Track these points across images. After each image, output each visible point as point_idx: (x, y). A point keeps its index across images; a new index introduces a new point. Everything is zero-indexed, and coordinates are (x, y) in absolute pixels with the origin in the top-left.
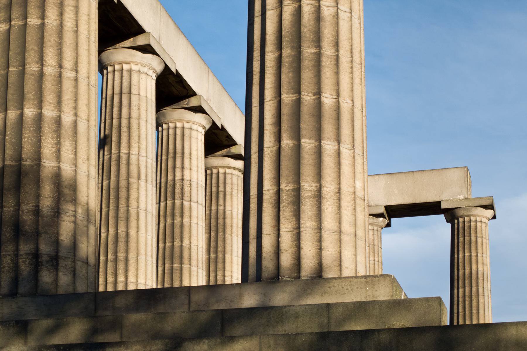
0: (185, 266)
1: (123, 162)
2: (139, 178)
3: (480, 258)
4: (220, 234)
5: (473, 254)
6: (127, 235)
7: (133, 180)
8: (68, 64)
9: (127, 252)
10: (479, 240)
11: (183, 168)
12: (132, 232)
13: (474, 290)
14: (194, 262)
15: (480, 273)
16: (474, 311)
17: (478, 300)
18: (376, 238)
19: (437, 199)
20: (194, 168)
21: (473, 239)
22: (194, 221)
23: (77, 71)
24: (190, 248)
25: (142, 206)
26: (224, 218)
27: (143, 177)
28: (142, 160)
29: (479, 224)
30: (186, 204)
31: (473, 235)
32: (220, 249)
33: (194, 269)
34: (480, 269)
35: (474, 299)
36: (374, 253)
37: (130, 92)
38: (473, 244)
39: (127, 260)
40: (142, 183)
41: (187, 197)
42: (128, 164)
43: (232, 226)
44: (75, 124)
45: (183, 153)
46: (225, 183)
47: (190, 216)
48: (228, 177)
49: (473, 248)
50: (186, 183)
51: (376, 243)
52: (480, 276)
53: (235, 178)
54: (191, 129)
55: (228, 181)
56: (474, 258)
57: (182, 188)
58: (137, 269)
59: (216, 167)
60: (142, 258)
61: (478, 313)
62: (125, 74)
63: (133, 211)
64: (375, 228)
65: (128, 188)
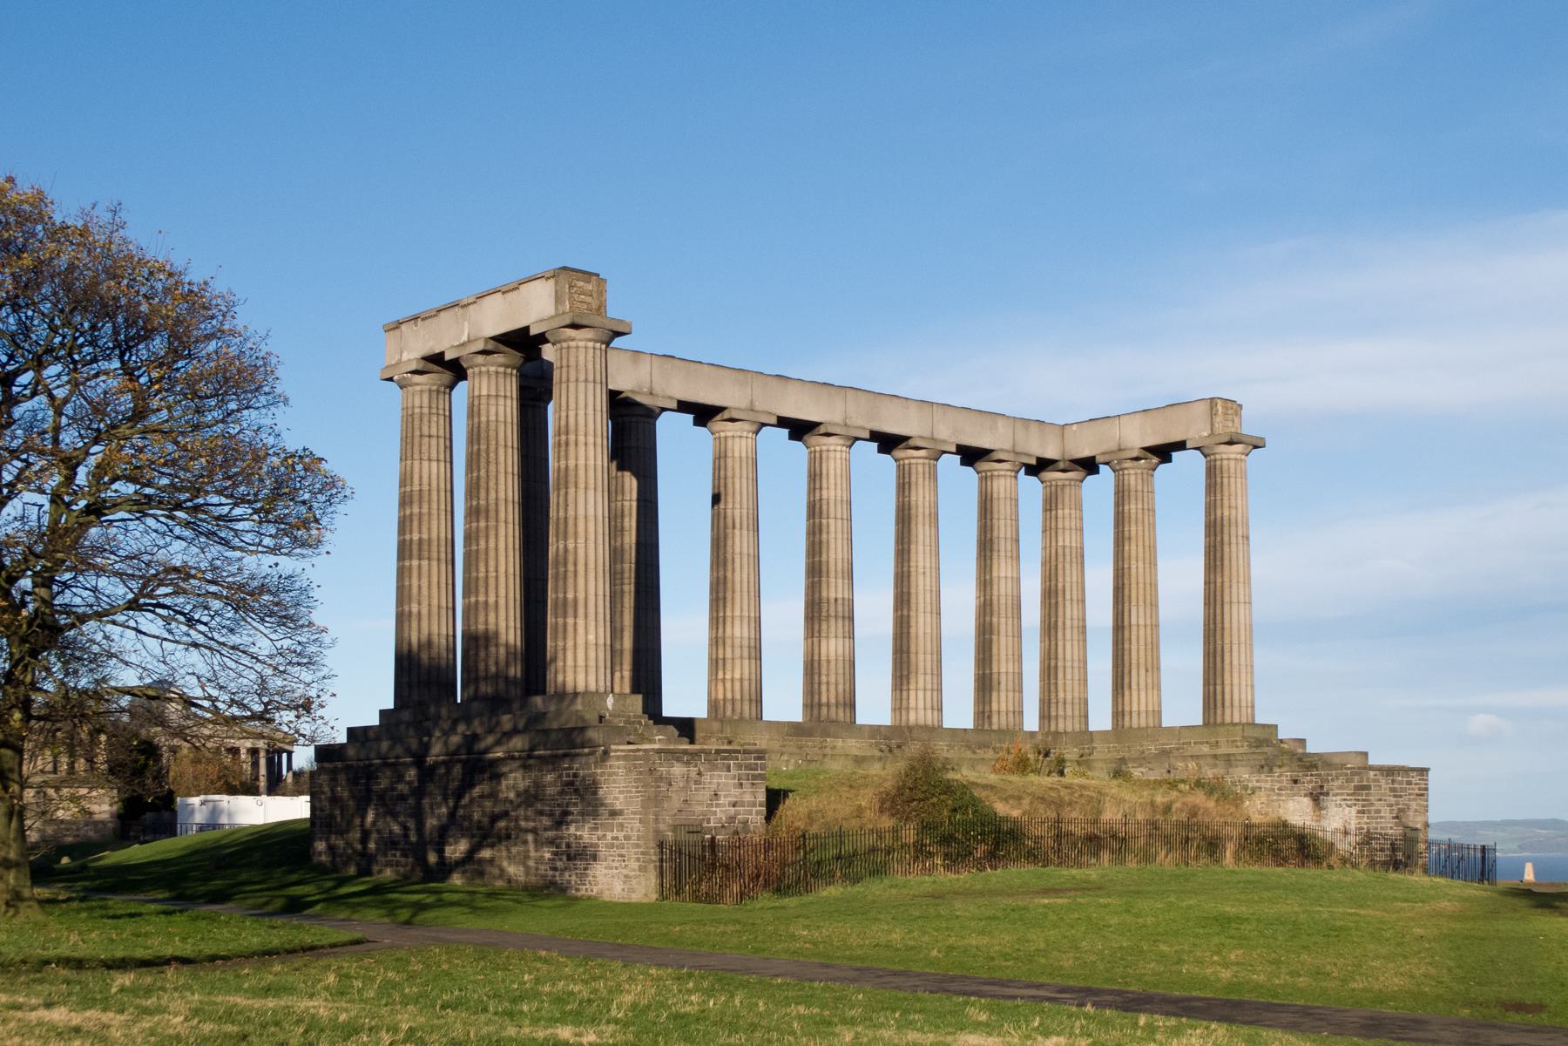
0: (824, 579)
1: (722, 516)
2: (734, 527)
3: (1226, 502)
4: (906, 524)
5: (1219, 498)
6: (725, 577)
7: (729, 531)
8: (492, 569)
9: (725, 593)
10: (1226, 480)
11: (821, 488)
12: (729, 575)
13: (1219, 539)
14: (832, 574)
15: (1226, 519)
16: (1218, 563)
17: (1222, 550)
18: (1140, 481)
20: (832, 487)
21: (1219, 480)
22: (832, 535)
23: (497, 571)
24: (828, 562)
25: (737, 550)
26: (909, 509)
27: (738, 526)
28: (737, 513)
29: (1225, 462)
30: (824, 521)
31: (1219, 476)
32: (906, 540)
33: (832, 580)
34: (1226, 513)
35: (1219, 549)
36: (1136, 500)
37: (726, 456)
38: (1218, 486)
39: (725, 598)
40: (737, 532)
41: (825, 515)
42: (725, 517)
43: (917, 516)
44: (497, 602)
45: (821, 475)
46: (910, 473)
47: (828, 533)
48: (913, 467)
49: (1218, 491)
50: (824, 502)
51: (1140, 488)
52: (1226, 523)
53: (920, 469)
54: (828, 451)
55: (913, 471)
56: (1219, 502)
57: (821, 507)
58: (733, 604)
59: (903, 459)
61: (1222, 565)
62: (722, 440)
63: (729, 556)
64: (1139, 471)
65: (725, 538)
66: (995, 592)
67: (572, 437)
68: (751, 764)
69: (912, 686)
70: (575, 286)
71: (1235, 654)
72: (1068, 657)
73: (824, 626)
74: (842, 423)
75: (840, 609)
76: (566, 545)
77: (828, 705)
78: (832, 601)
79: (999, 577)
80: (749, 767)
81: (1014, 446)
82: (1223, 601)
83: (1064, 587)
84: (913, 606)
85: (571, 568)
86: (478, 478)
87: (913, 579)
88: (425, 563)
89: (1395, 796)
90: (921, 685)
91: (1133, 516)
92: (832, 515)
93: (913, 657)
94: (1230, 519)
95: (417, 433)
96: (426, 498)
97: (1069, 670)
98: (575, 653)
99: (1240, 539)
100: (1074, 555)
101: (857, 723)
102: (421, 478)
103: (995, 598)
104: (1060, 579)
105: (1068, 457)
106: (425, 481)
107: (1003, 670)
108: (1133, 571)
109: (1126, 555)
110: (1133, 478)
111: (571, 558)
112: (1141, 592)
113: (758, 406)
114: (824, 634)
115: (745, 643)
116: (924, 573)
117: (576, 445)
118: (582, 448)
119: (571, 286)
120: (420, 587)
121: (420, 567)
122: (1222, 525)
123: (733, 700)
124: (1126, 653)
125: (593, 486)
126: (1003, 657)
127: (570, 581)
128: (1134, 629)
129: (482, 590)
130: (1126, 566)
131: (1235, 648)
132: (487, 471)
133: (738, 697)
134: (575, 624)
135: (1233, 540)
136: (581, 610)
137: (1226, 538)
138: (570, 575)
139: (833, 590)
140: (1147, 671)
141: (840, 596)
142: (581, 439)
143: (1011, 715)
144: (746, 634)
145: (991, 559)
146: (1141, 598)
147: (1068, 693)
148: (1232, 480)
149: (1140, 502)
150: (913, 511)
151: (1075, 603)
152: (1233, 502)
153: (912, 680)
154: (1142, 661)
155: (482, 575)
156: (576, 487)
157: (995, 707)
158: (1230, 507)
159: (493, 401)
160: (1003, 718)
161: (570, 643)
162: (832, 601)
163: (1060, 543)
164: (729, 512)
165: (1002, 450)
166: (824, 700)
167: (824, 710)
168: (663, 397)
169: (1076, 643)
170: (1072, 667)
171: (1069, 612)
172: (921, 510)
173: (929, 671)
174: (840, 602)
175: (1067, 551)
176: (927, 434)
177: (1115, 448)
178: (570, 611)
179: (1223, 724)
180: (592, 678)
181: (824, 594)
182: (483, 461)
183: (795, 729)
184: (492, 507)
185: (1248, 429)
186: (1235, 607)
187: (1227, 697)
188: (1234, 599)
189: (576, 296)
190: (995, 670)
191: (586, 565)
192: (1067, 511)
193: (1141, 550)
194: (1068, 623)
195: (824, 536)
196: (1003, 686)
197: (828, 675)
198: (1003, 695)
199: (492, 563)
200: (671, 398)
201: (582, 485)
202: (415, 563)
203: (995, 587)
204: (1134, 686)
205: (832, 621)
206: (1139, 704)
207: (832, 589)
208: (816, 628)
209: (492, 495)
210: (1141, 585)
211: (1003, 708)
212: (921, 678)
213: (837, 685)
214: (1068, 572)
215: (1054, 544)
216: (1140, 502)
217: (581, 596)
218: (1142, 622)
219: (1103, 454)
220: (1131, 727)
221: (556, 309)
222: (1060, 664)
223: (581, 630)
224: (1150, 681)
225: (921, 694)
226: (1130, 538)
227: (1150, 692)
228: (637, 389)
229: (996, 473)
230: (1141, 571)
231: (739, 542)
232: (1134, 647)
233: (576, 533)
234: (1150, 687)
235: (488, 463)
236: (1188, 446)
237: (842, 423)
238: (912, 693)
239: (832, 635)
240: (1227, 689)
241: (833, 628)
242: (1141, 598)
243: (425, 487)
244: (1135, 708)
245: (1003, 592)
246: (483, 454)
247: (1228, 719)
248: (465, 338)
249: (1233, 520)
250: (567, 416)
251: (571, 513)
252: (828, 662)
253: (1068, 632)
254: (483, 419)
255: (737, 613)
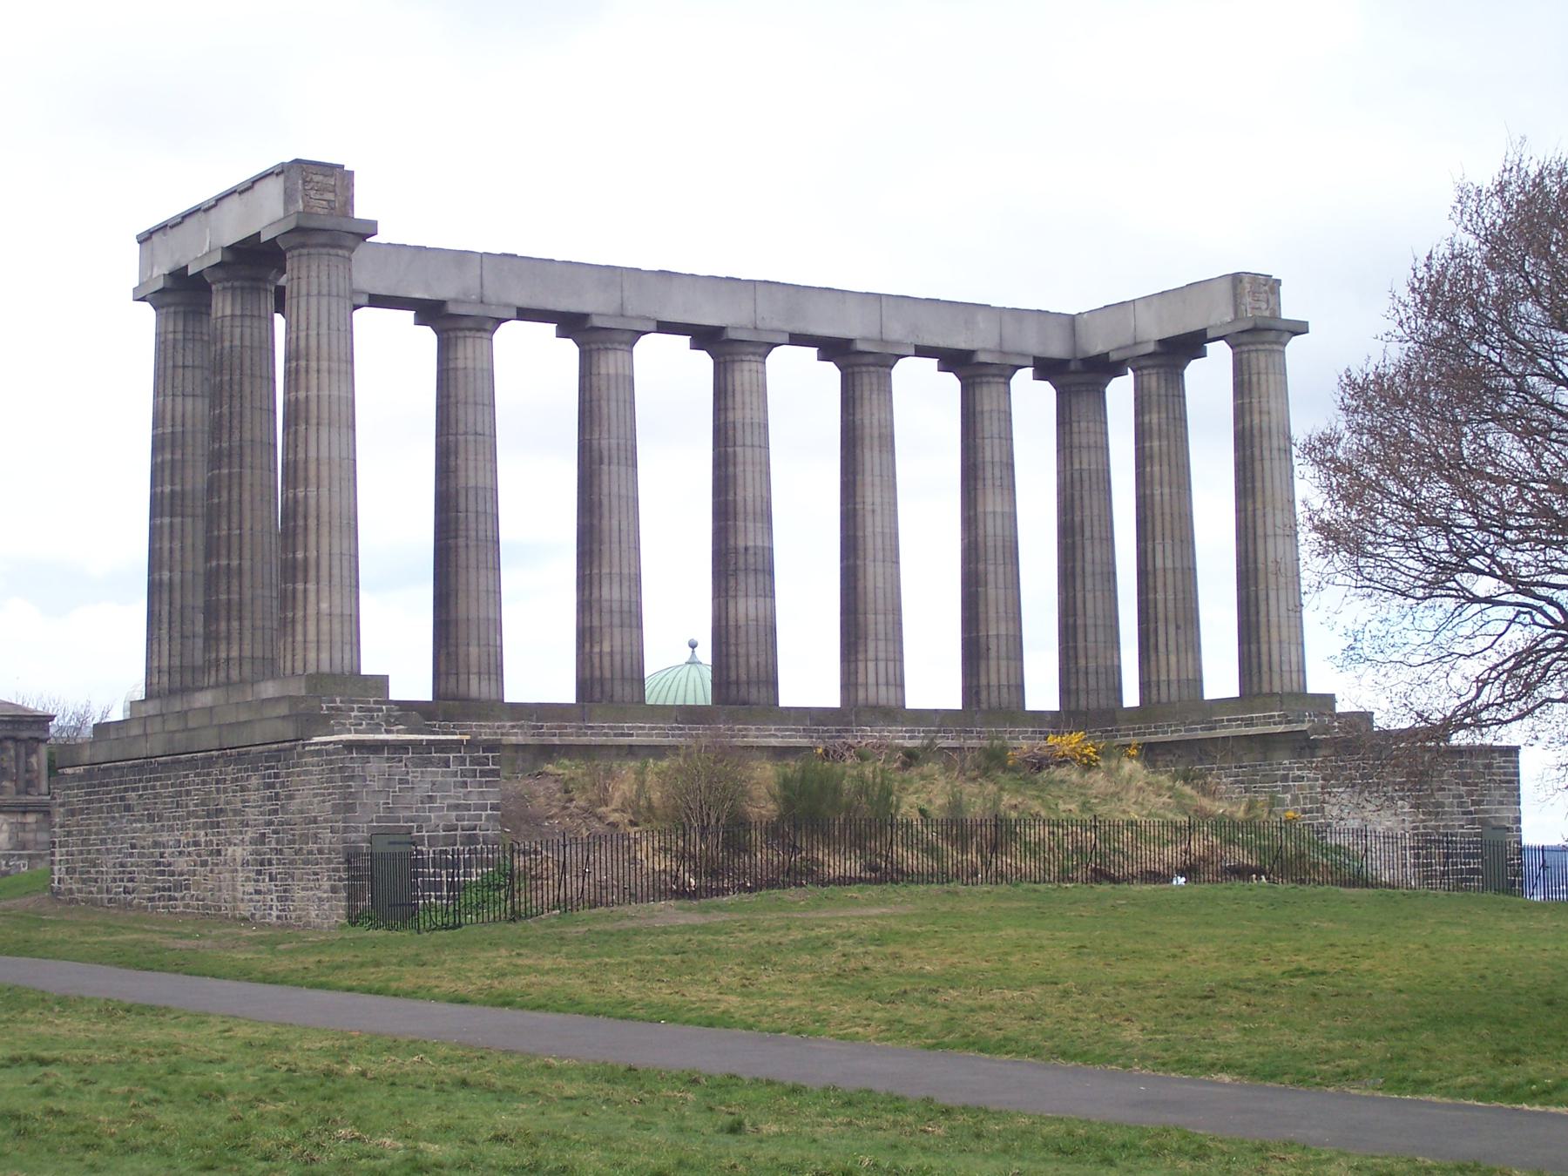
2: (601, 462)
7: (595, 467)
8: (235, 525)
10: (1254, 379)
13: (1248, 453)
17: (1253, 468)
19: (1200, 327)
27: (606, 460)
30: (730, 450)
34: (1256, 421)
35: (1249, 467)
41: (730, 443)
52: (1256, 432)
60: (605, 547)
66: (981, 532)
67: (303, 363)
68: (479, 757)
69: (861, 656)
70: (311, 180)
71: (1273, 602)
72: (1090, 612)
73: (732, 583)
74: (750, 326)
75: (751, 560)
76: (295, 495)
77: (737, 682)
78: (743, 550)
79: (985, 513)
80: (474, 761)
81: (1001, 344)
82: (1255, 534)
83: (1082, 522)
84: (861, 553)
85: (301, 522)
86: (221, 415)
87: (859, 519)
88: (178, 520)
89: (1465, 784)
90: (871, 654)
91: (1155, 427)
92: (739, 441)
93: (861, 618)
94: (1261, 429)
95: (170, 363)
96: (179, 442)
97: (1091, 630)
98: (305, 626)
99: (1275, 453)
100: (1094, 479)
101: (781, 704)
102: (173, 418)
103: (980, 539)
104: (1078, 513)
105: (1080, 356)
106: (179, 420)
107: (992, 632)
108: (1157, 498)
109: (1148, 478)
110: (1154, 379)
111: (301, 509)
112: (1168, 525)
113: (631, 310)
114: (732, 593)
115: (616, 607)
116: (873, 511)
117: (307, 371)
118: (313, 375)
119: (305, 182)
120: (171, 551)
121: (171, 525)
122: (1252, 435)
123: (602, 679)
124: (1151, 605)
125: (326, 421)
126: (992, 613)
127: (300, 538)
128: (1160, 574)
129: (224, 552)
130: (1148, 492)
131: (1272, 594)
132: (230, 407)
133: (607, 675)
134: (305, 590)
135: (1266, 454)
136: (312, 573)
137: (1257, 452)
138: (300, 530)
139: (747, 537)
140: (1178, 627)
141: (751, 544)
142: (313, 365)
143: (1004, 690)
144: (616, 596)
145: (976, 489)
146: (1168, 533)
147: (1090, 660)
148: (1263, 377)
149: (1163, 409)
150: (858, 433)
151: (1097, 542)
152: (1264, 405)
153: (861, 648)
154: (1171, 615)
155: (224, 533)
156: (307, 423)
157: (983, 681)
158: (1260, 412)
159: (238, 322)
160: (994, 694)
161: (300, 614)
162: (742, 550)
163: (1077, 466)
164: (595, 443)
165: (985, 350)
166: (733, 676)
167: (733, 689)
168: (498, 305)
169: (1098, 594)
170: (1096, 626)
171: (1091, 553)
172: (867, 431)
173: (881, 636)
174: (751, 551)
175: (1085, 475)
176: (875, 334)
177: (1130, 341)
178: (300, 576)
179: (1260, 694)
180: (325, 656)
181: (732, 542)
182: (226, 394)
183: (689, 714)
184: (236, 451)
185: (1289, 312)
186: (1270, 541)
187: (1265, 658)
188: (1270, 531)
189: (312, 193)
190: (983, 633)
191: (318, 517)
192: (1083, 425)
193: (1165, 468)
194: (1089, 568)
195: (731, 469)
196: (993, 653)
197: (737, 645)
198: (993, 663)
199: (235, 519)
200: (507, 306)
201: (313, 421)
202: (167, 520)
203: (981, 526)
204: (1162, 648)
205: (741, 576)
206: (1168, 671)
207: (751, 536)
208: (723, 584)
209: (236, 437)
210: (1168, 518)
211: (994, 681)
212: (871, 645)
213: (748, 656)
214: (1086, 502)
215: (1068, 467)
216: (1163, 409)
217: (312, 554)
218: (1169, 564)
219: (1118, 349)
220: (1159, 702)
221: (286, 209)
222: (1080, 622)
223: (312, 597)
224: (1182, 641)
225: (871, 665)
226: (1151, 457)
227: (1182, 655)
228: (461, 297)
229: (978, 380)
230: (1166, 498)
231: (610, 477)
232: (1160, 596)
233: (306, 479)
234: (1182, 648)
235: (231, 397)
236: (1210, 335)
237: (750, 326)
238: (861, 665)
239: (741, 593)
240: (1264, 648)
241: (742, 586)
242: (1168, 533)
243: (179, 429)
244: (1163, 677)
245: (990, 530)
246: (227, 387)
247: (1266, 689)
248: (206, 249)
249: (1265, 429)
250: (297, 338)
251: (301, 455)
252: (737, 627)
253: (1089, 581)
254: (227, 344)
255: (605, 570)
